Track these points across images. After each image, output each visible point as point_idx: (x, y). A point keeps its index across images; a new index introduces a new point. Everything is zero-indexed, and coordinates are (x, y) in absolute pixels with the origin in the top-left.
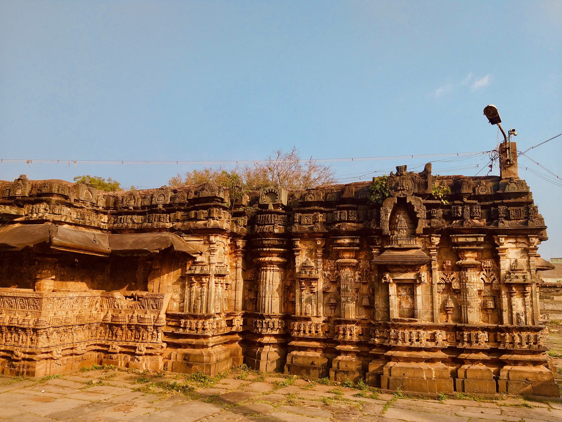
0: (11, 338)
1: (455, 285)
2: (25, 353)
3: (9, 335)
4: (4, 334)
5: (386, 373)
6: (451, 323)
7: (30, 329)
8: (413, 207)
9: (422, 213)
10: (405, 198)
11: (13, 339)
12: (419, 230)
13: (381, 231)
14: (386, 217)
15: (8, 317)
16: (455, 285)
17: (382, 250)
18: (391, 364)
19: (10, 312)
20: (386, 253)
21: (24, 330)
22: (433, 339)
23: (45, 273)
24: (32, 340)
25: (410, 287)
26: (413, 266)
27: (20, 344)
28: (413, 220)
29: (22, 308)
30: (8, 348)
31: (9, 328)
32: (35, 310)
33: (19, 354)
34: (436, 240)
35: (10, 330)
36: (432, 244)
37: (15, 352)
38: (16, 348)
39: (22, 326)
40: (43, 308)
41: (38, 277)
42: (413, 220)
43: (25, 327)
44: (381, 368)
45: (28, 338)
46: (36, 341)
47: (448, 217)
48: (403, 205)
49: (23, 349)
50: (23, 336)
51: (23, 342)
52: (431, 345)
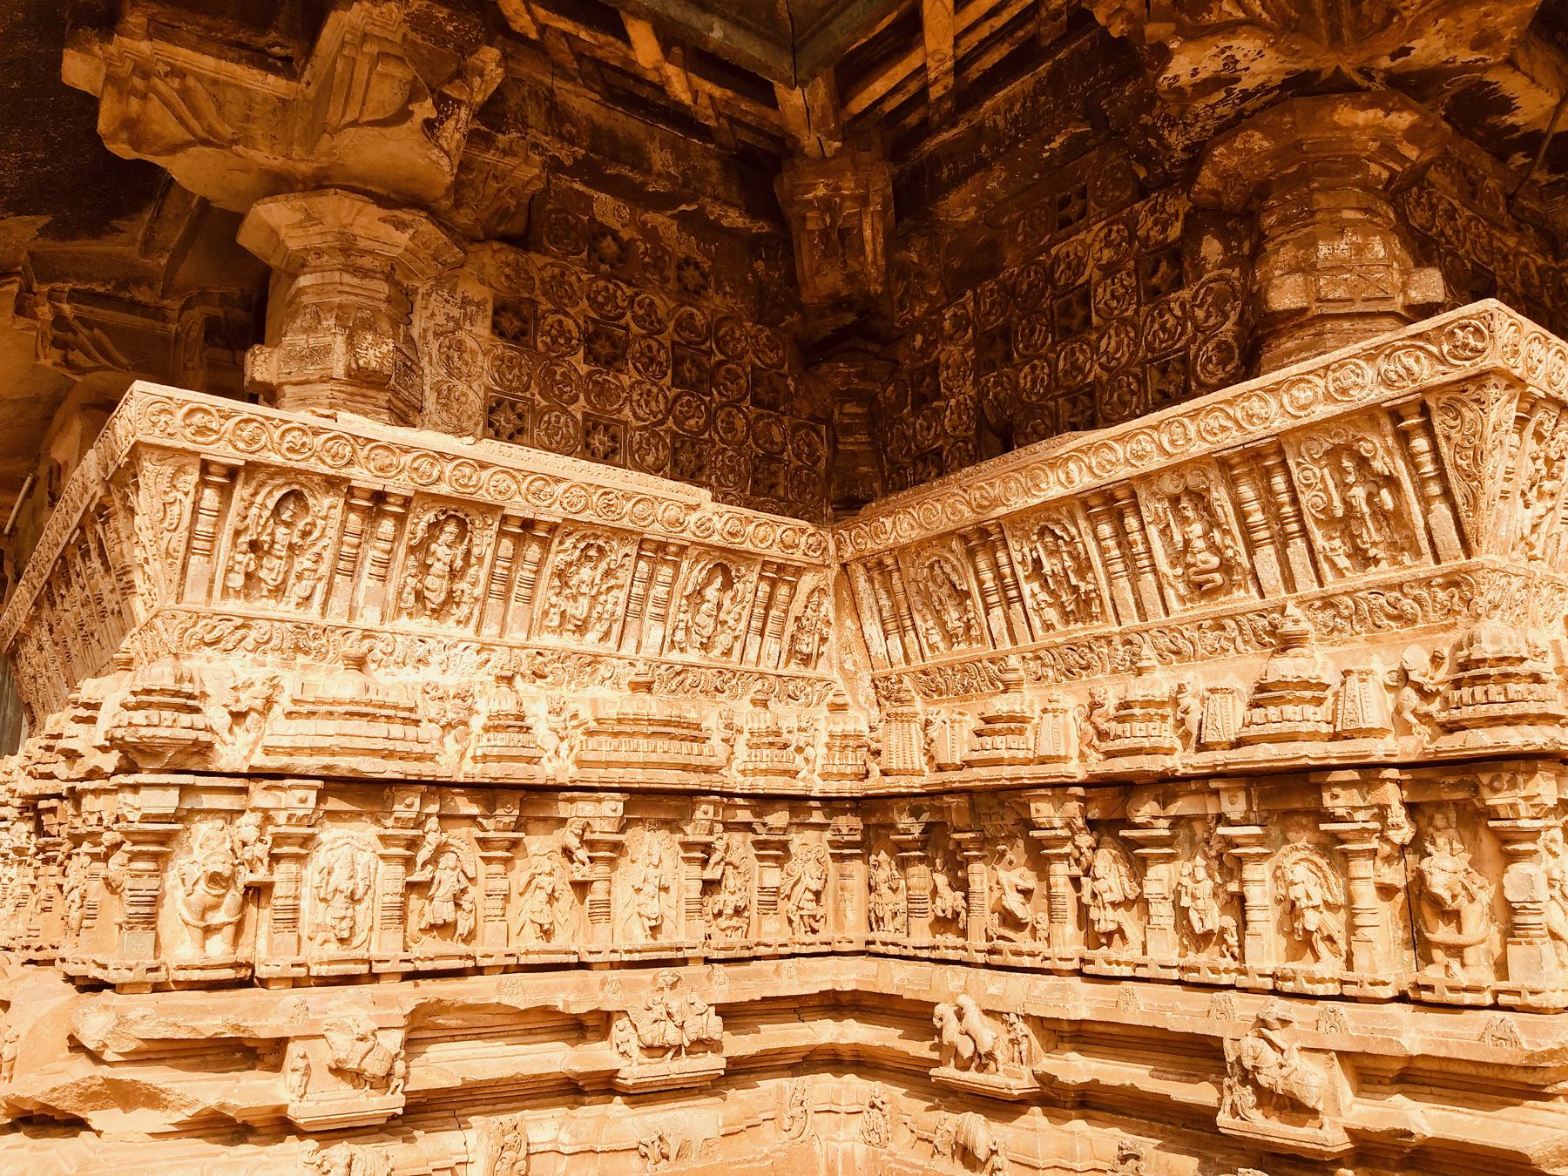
0: (1139, 903)
2: (1368, 1072)
3: (1110, 875)
4: (1060, 871)
7: (1369, 771)
11: (1163, 913)
15: (1071, 699)
19: (1074, 664)
21: (1288, 793)
23: (1338, 267)
24: (1421, 906)
27: (1267, 950)
29: (1200, 589)
30: (1143, 1007)
31: (1112, 801)
32: (1384, 572)
33: (1317, 1080)
35: (1104, 828)
37: (1244, 1046)
38: (1244, 1008)
39: (1262, 755)
40: (1486, 520)
41: (1286, 295)
43: (1311, 752)
45: (1366, 895)
46: (1478, 926)
49: (1354, 1027)
50: (1289, 872)
51: (1303, 944)
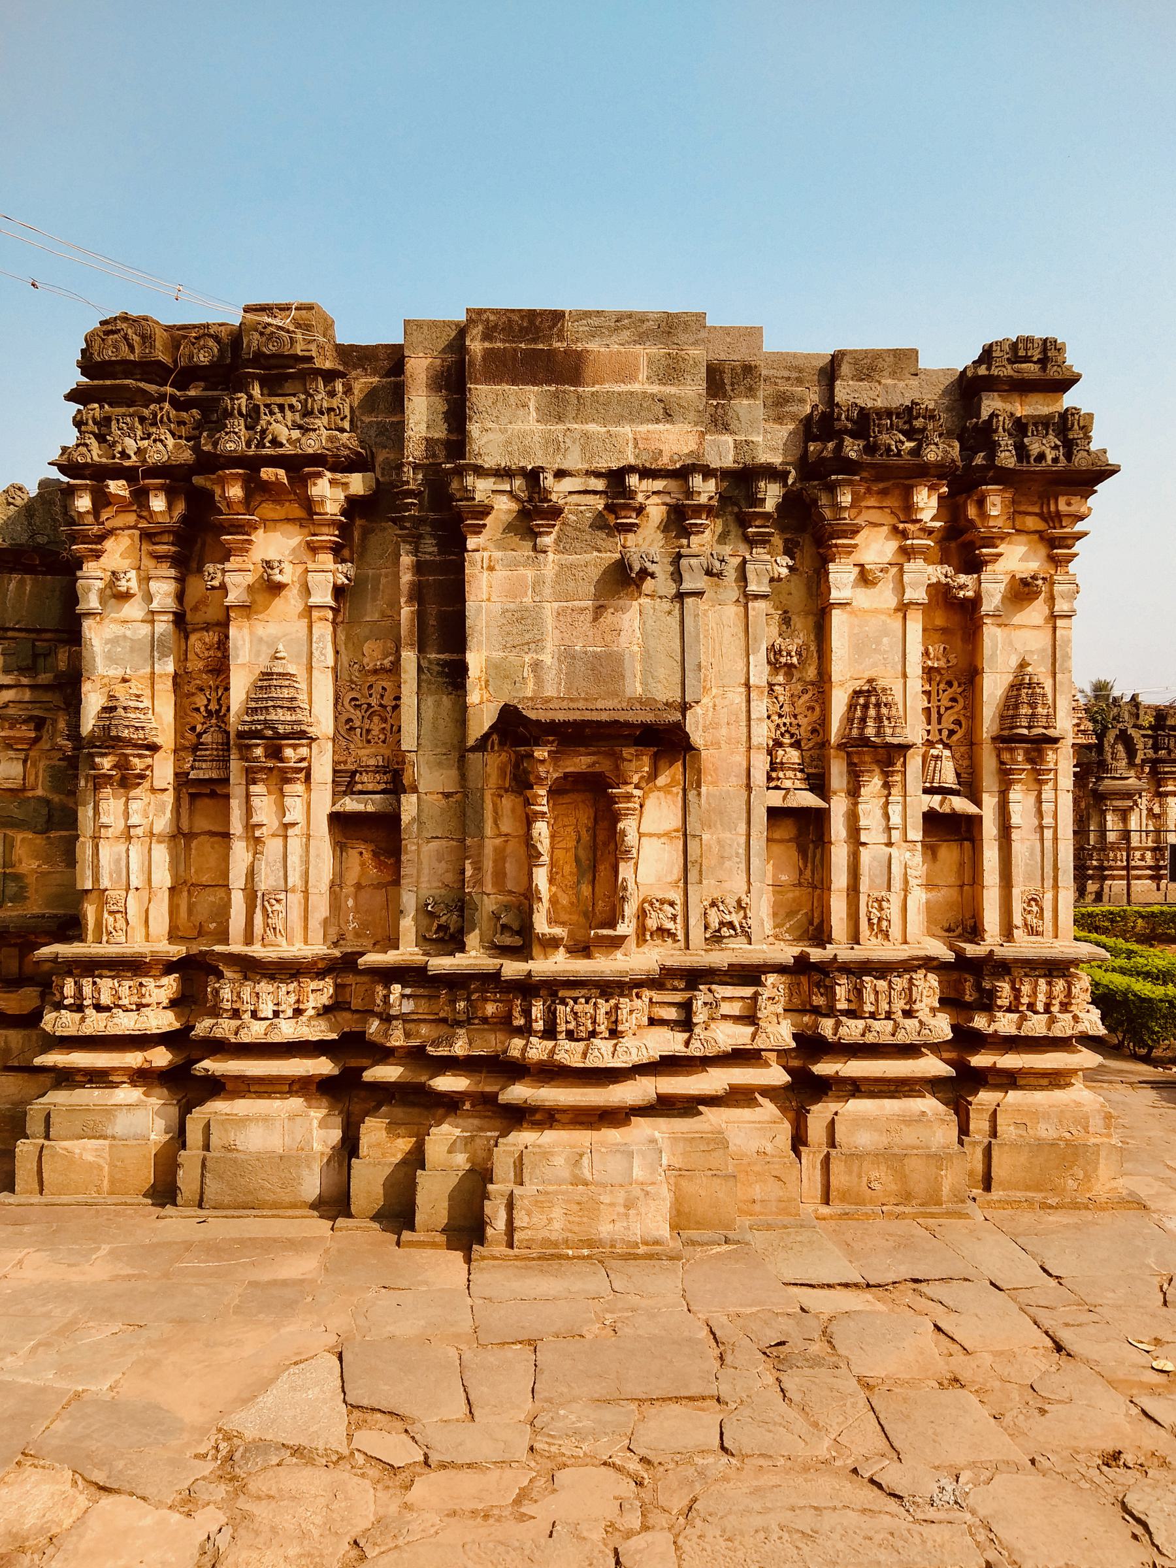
1: (1157, 810)
5: (1106, 889)
6: (1150, 844)
8: (1133, 738)
9: (1140, 746)
10: (1126, 730)
12: (1138, 761)
13: (1105, 760)
14: (1107, 748)
16: (1157, 810)
17: (1100, 779)
18: (1108, 882)
20: (1107, 782)
22: (1143, 859)
25: (1124, 815)
26: (1128, 795)
28: (1131, 752)
34: (1147, 770)
36: (1143, 772)
42: (1131, 752)
44: (1102, 887)
47: (1156, 748)
48: (1124, 738)
52: (1143, 863)
